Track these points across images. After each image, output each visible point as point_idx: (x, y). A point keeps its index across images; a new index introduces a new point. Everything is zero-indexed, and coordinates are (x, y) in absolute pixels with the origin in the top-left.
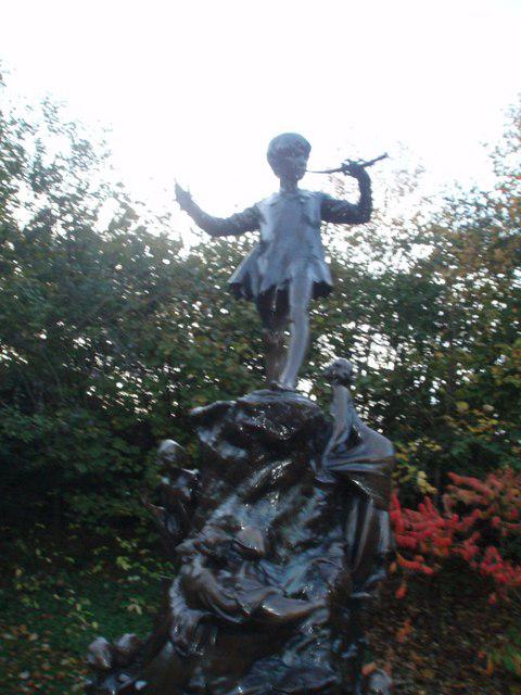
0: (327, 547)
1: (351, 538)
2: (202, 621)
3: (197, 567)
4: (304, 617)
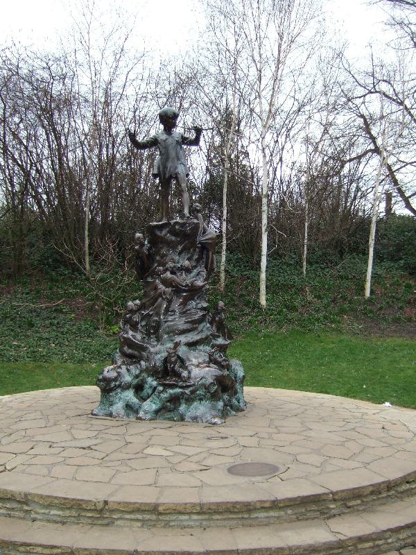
3: (168, 274)
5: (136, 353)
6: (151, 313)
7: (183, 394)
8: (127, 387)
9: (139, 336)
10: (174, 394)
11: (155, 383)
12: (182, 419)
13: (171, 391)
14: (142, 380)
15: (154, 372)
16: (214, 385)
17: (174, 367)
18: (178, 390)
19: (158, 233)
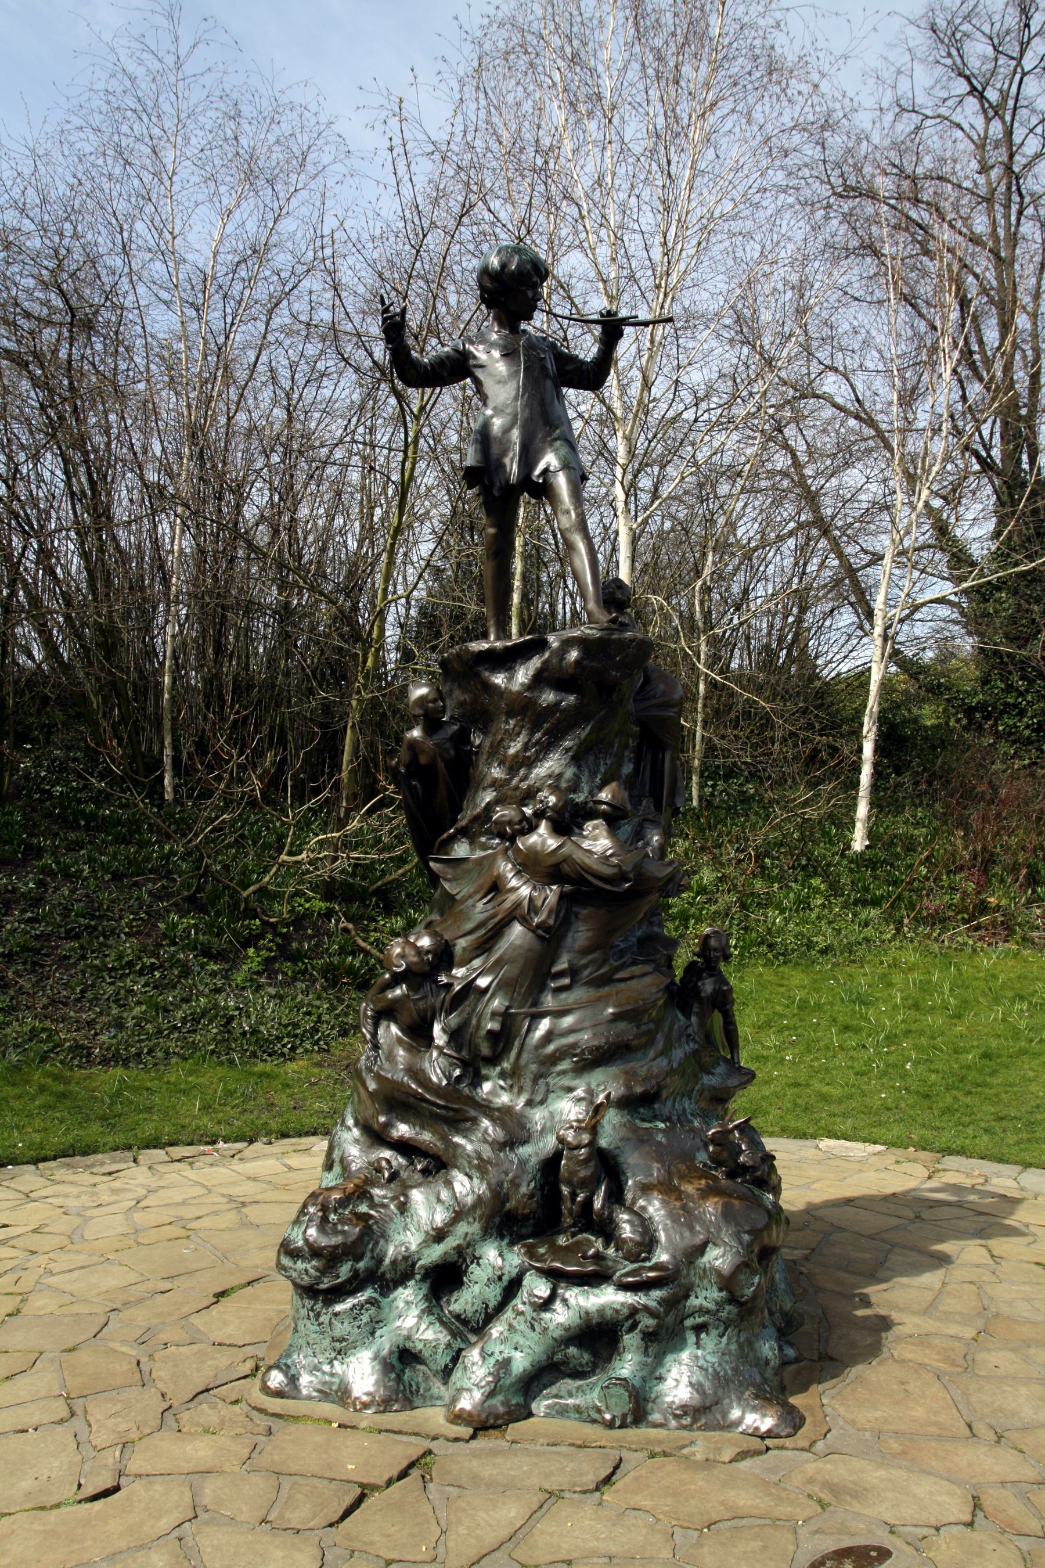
2: (562, 896)
5: (426, 1136)
6: (483, 982)
9: (436, 1069)
10: (601, 1311)
11: (515, 1258)
14: (459, 1250)
17: (589, 1202)
19: (499, 680)
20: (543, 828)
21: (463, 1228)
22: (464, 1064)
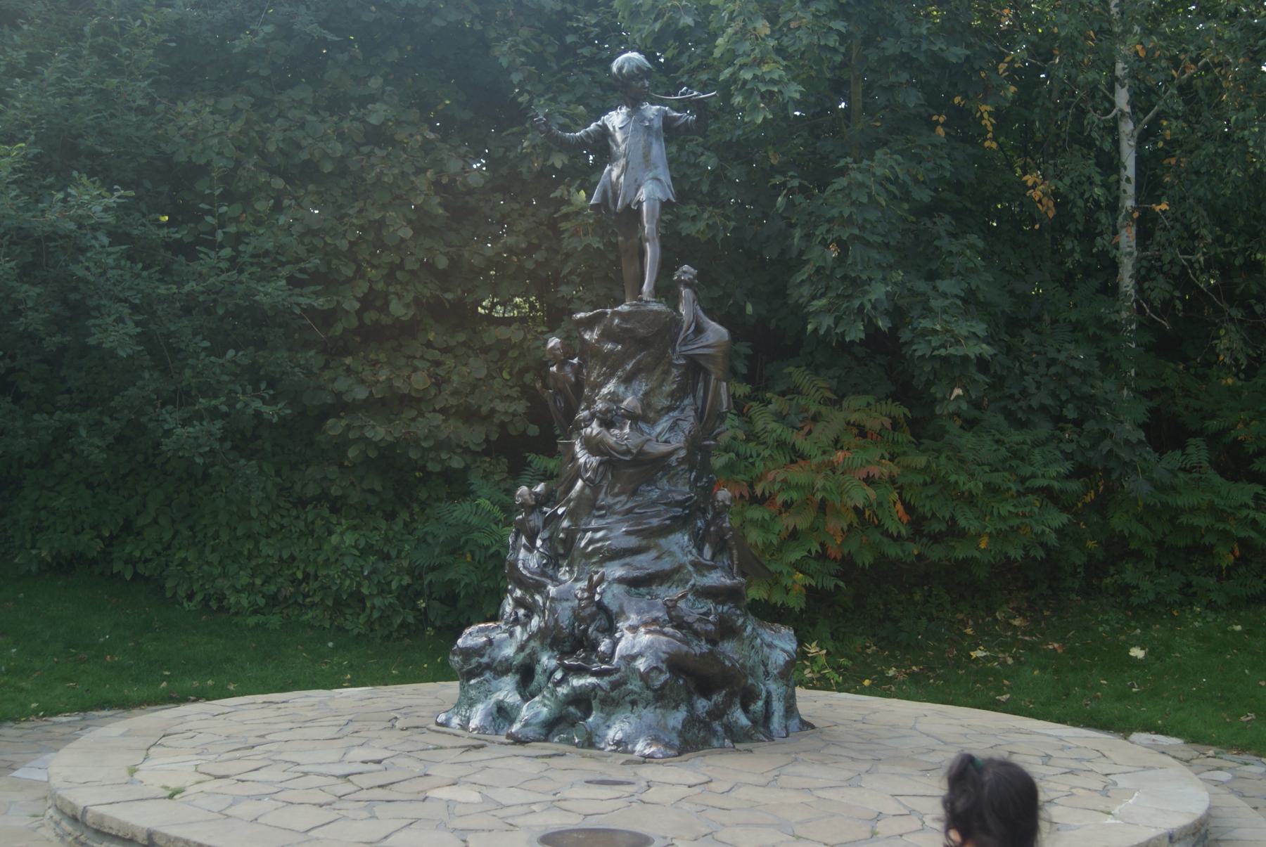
0: (683, 410)
1: (699, 403)
2: (601, 463)
3: (594, 429)
4: (671, 453)
7: (595, 687)
8: (502, 669)
12: (590, 742)
13: (576, 682)
15: (553, 638)
16: (661, 671)
17: (586, 630)
18: (591, 680)
20: (595, 424)
21: (532, 644)
22: (549, 558)
